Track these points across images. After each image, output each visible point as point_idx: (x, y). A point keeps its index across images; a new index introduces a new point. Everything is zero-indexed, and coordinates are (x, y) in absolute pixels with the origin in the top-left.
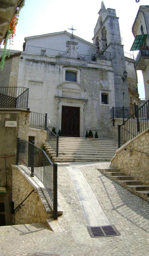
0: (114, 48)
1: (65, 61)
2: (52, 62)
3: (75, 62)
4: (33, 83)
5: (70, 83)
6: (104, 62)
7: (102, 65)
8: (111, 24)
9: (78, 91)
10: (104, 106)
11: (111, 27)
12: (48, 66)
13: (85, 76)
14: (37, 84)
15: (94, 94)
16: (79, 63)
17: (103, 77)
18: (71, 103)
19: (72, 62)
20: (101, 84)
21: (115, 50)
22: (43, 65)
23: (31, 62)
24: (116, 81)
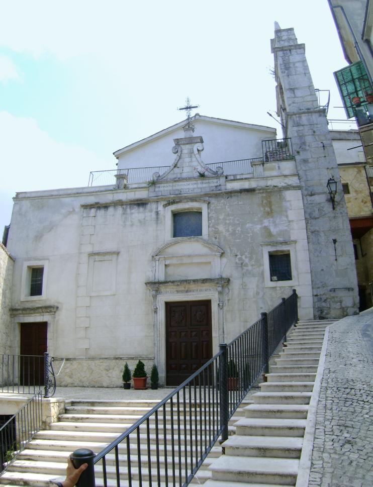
0: (298, 125)
1: (170, 188)
2: (137, 200)
3: (195, 186)
4: (97, 258)
5: (182, 241)
6: (272, 169)
7: (267, 178)
8: (285, 66)
9: (203, 260)
10: (278, 289)
11: (286, 72)
12: (131, 210)
13: (221, 217)
14: (107, 257)
15: (247, 261)
16: (204, 185)
17: (271, 210)
18: (187, 291)
19: (189, 187)
20: (266, 229)
21: (301, 128)
22: (120, 210)
23: (93, 210)
24: (309, 211)
